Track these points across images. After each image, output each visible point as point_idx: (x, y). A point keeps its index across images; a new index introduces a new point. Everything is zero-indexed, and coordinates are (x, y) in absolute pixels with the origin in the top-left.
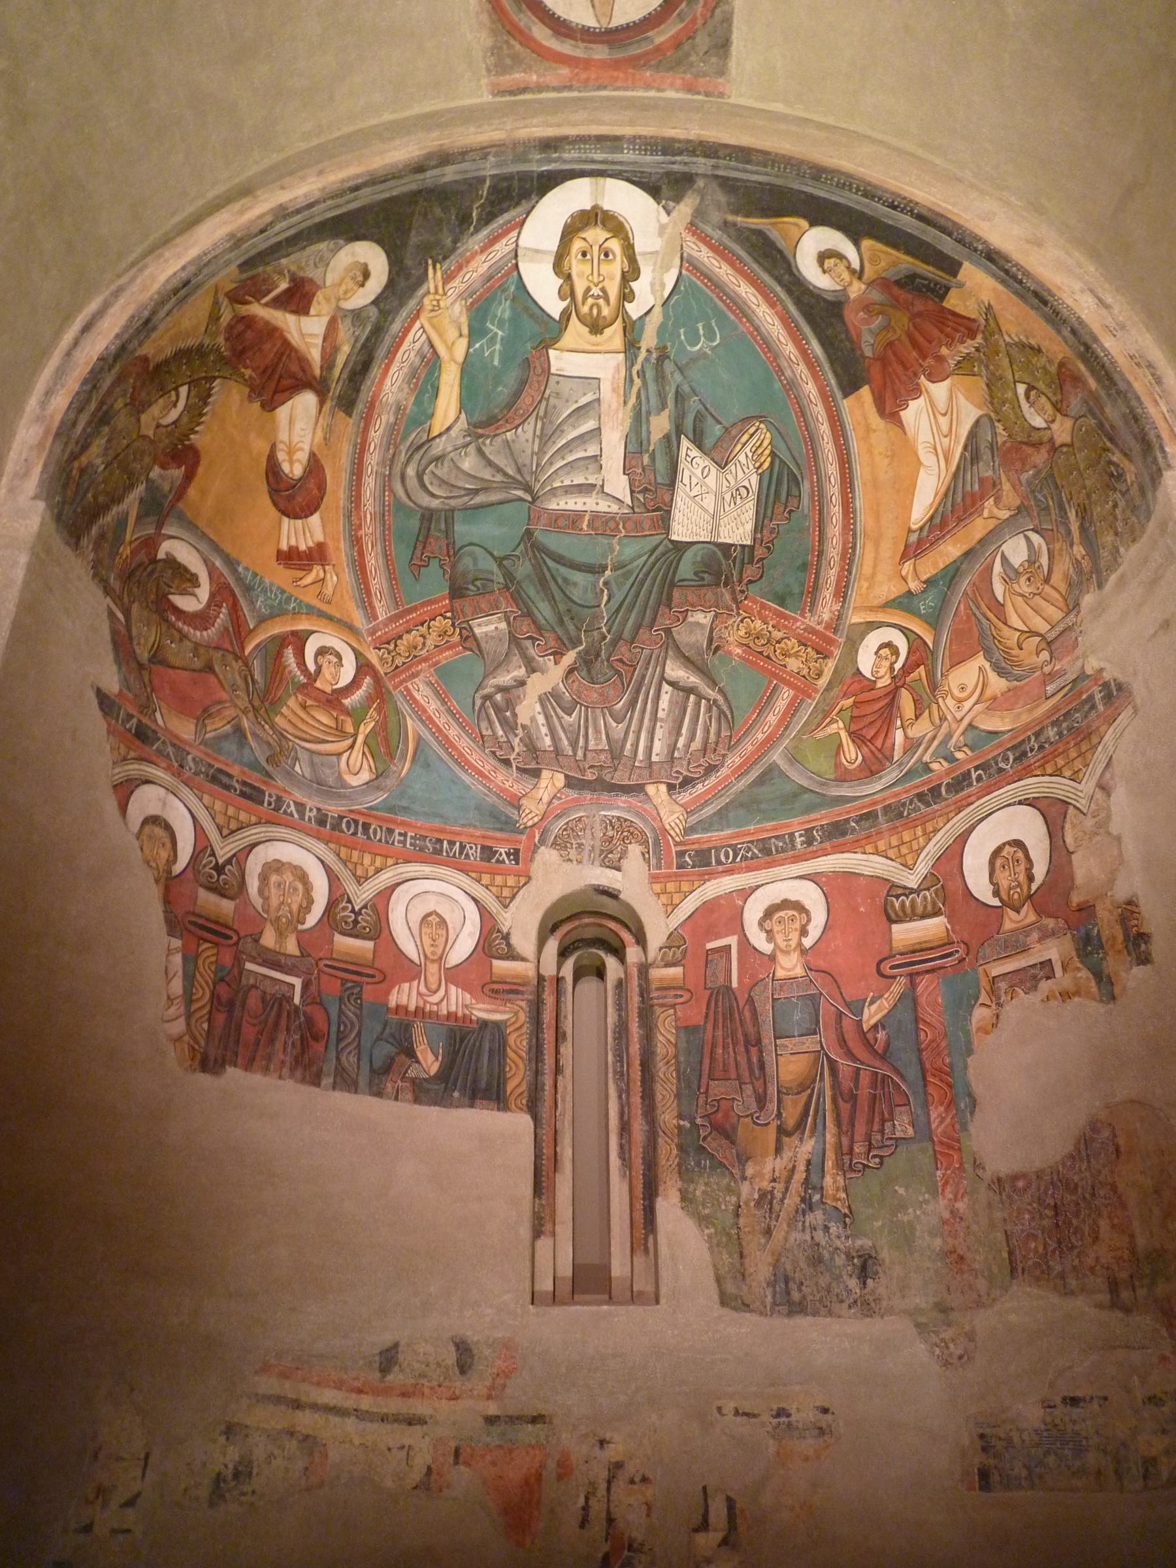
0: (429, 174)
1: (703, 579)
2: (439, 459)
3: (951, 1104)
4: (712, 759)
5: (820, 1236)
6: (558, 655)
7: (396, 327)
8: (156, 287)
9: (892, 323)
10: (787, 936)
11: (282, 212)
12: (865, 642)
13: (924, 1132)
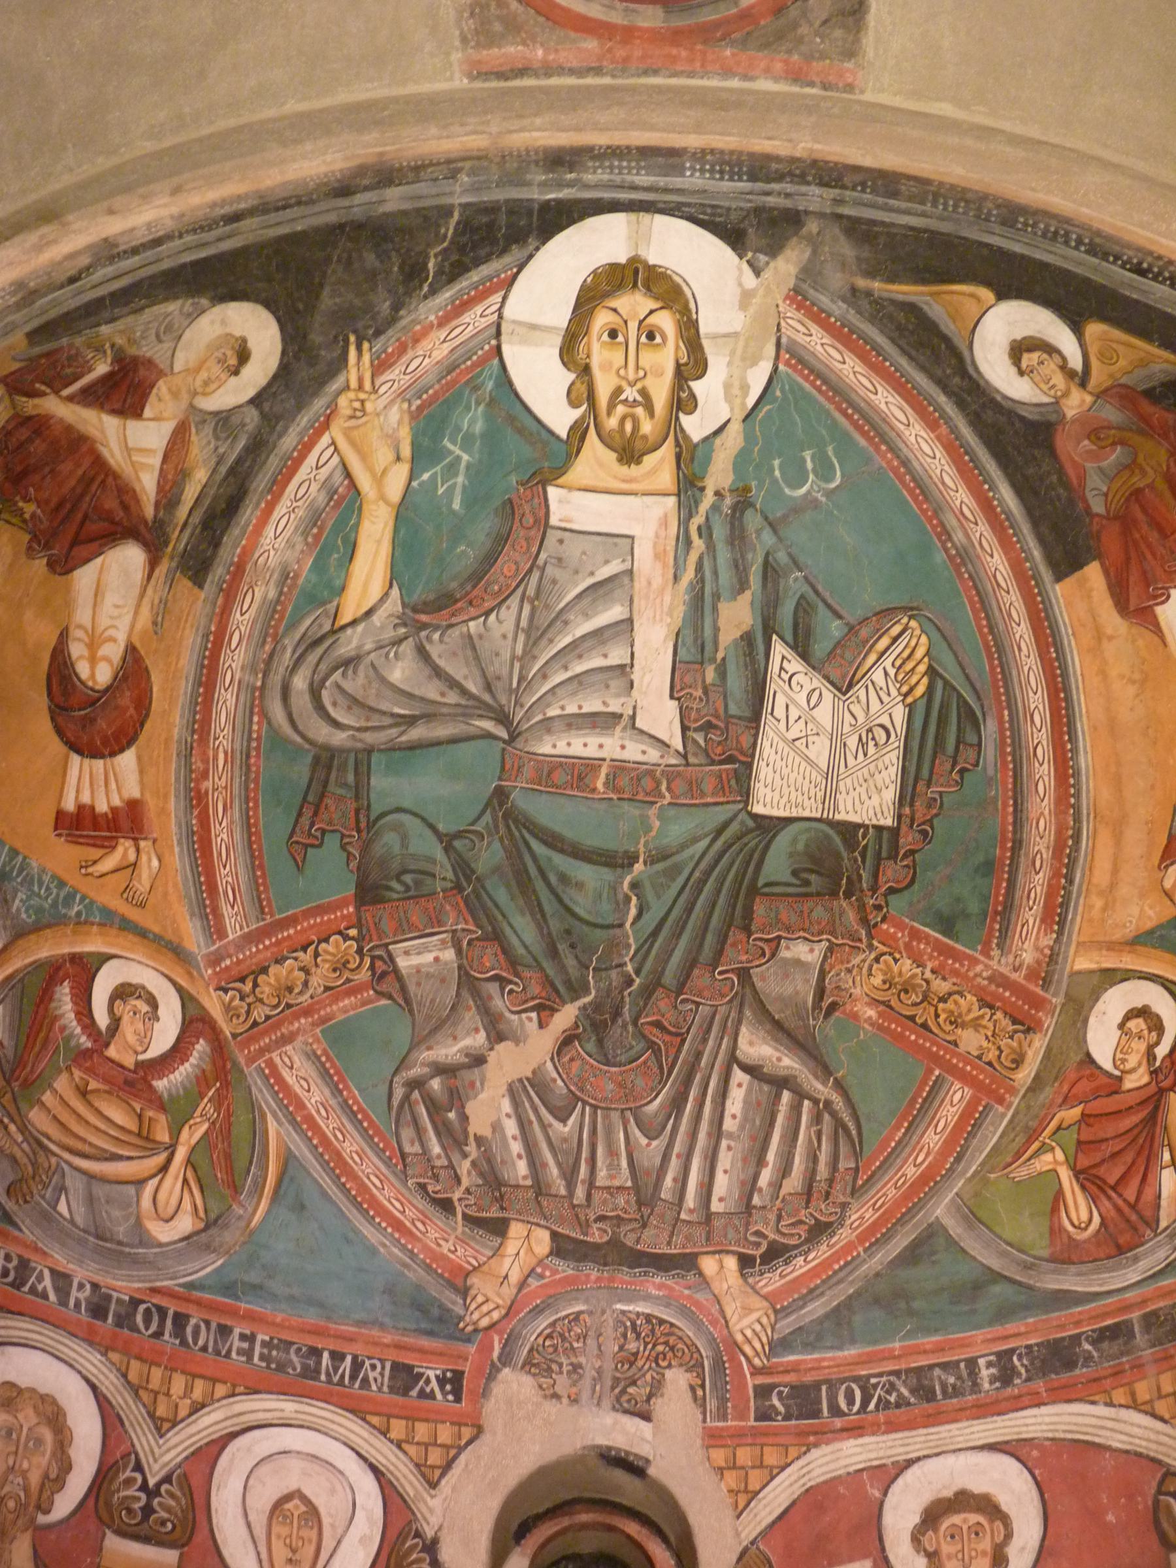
0: (359, 198)
1: (807, 883)
2: (349, 663)
4: (822, 1210)
6: (545, 1010)
7: (289, 442)
9: (1140, 459)
12: (1100, 1006)
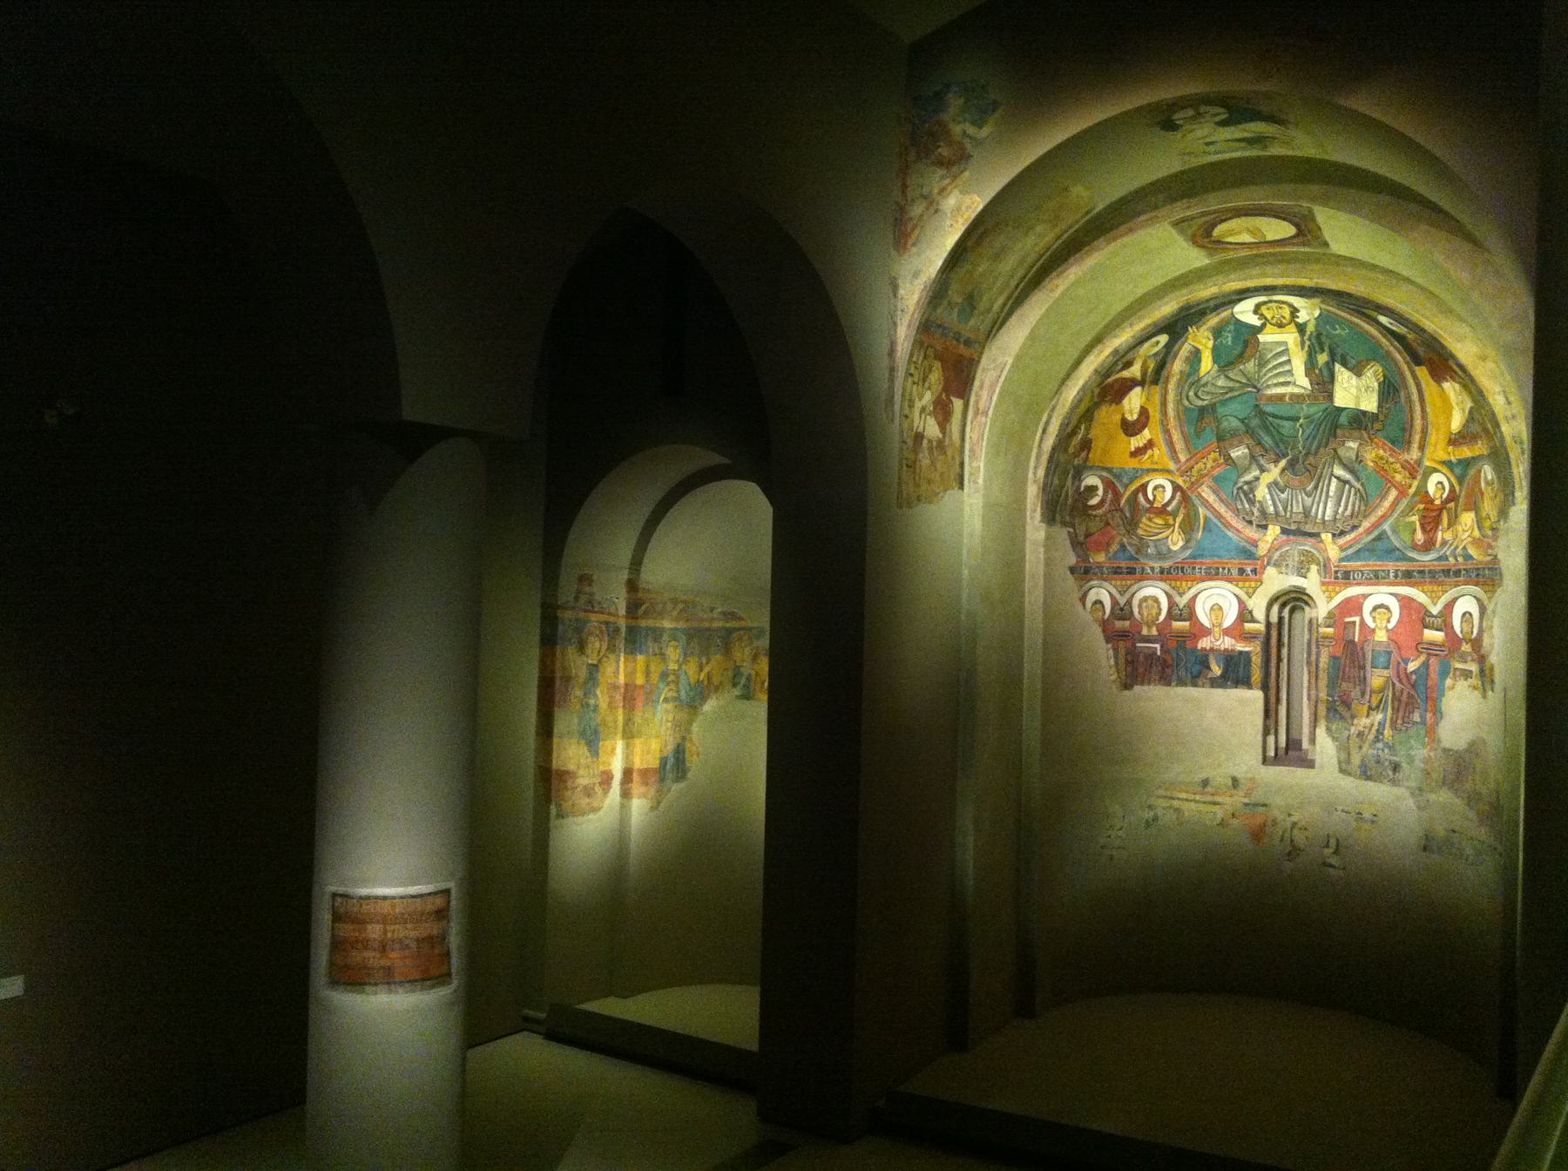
2: (1203, 386)
4: (1356, 522)
6: (1276, 462)
7: (1176, 347)
8: (1068, 404)
11: (1116, 352)
13: (1424, 722)
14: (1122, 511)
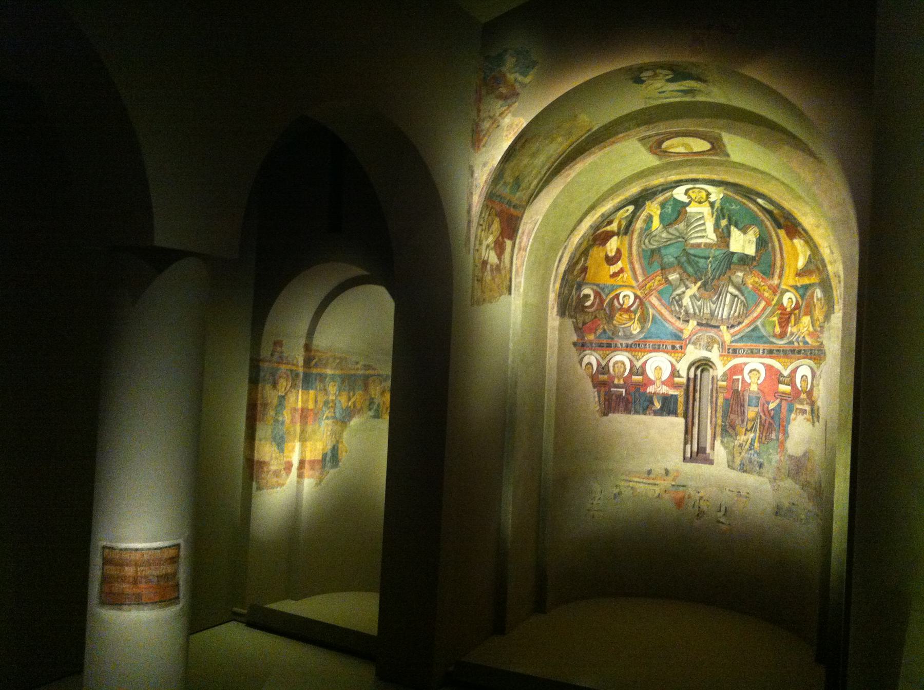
2: (655, 236)
3: (784, 434)
4: (740, 320)
5: (752, 456)
6: (695, 283)
7: (638, 214)
8: (574, 246)
10: (754, 379)
11: (603, 215)
13: (778, 439)
14: (605, 310)
